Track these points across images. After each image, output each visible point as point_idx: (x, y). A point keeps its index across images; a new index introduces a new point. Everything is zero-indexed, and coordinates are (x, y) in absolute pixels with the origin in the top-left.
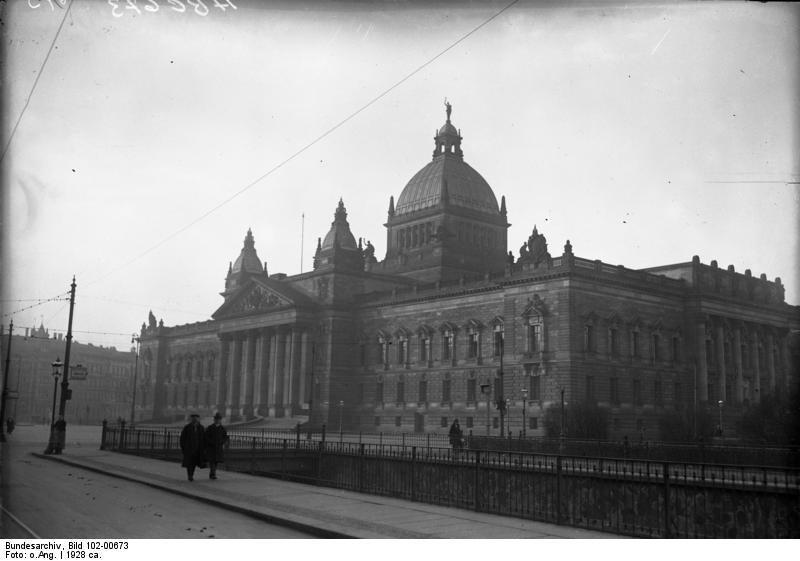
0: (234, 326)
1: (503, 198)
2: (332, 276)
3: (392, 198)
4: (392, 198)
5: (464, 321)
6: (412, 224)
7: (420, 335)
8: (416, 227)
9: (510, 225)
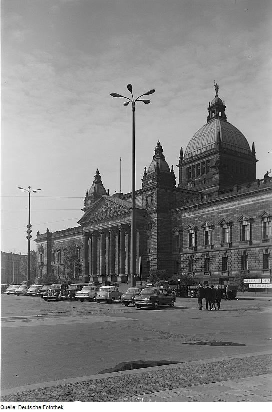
0: (92, 228)
1: (254, 143)
2: (155, 192)
3: (182, 148)
4: (182, 148)
5: (260, 212)
6: (195, 163)
7: (222, 225)
8: (199, 165)
9: (258, 161)
